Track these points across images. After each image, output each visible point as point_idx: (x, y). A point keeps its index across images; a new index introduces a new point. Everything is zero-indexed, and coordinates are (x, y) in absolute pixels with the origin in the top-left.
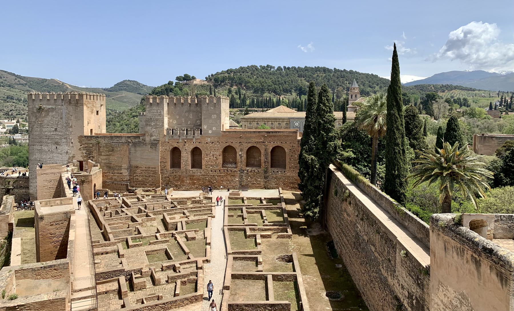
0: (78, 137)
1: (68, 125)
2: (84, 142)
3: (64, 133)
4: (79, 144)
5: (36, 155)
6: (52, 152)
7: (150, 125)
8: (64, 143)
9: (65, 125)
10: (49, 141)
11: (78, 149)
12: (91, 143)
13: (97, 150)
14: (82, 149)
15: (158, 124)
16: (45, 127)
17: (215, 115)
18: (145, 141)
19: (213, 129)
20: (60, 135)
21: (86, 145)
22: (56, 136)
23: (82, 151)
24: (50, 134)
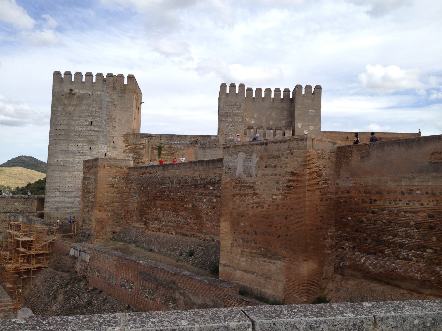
0: (124, 135)
1: (110, 118)
2: (131, 142)
3: (103, 128)
4: (124, 144)
5: (58, 158)
6: (83, 154)
7: (225, 121)
8: (102, 142)
9: (105, 118)
10: (79, 139)
11: (122, 151)
12: (141, 144)
13: (150, 153)
14: (127, 151)
15: (237, 120)
16: (76, 120)
17: (313, 111)
18: (218, 142)
19: (310, 128)
20: (97, 131)
21: (134, 146)
22: (90, 132)
23: (127, 154)
24: (81, 129)
